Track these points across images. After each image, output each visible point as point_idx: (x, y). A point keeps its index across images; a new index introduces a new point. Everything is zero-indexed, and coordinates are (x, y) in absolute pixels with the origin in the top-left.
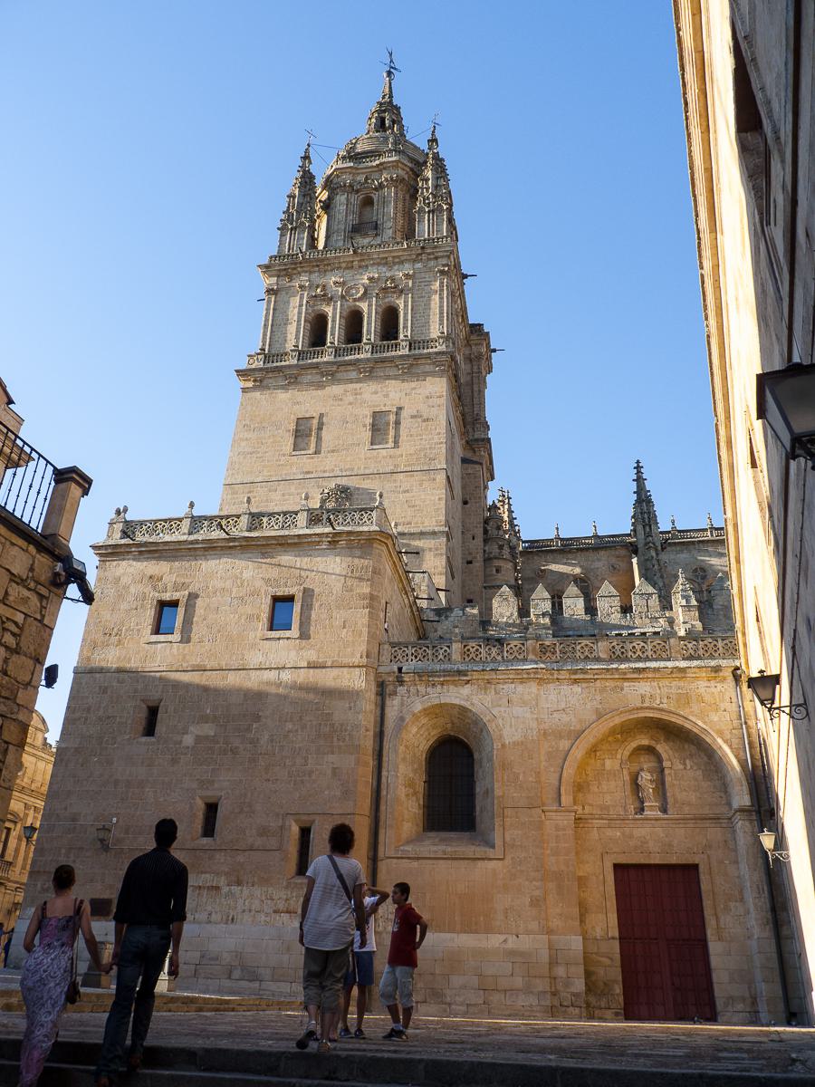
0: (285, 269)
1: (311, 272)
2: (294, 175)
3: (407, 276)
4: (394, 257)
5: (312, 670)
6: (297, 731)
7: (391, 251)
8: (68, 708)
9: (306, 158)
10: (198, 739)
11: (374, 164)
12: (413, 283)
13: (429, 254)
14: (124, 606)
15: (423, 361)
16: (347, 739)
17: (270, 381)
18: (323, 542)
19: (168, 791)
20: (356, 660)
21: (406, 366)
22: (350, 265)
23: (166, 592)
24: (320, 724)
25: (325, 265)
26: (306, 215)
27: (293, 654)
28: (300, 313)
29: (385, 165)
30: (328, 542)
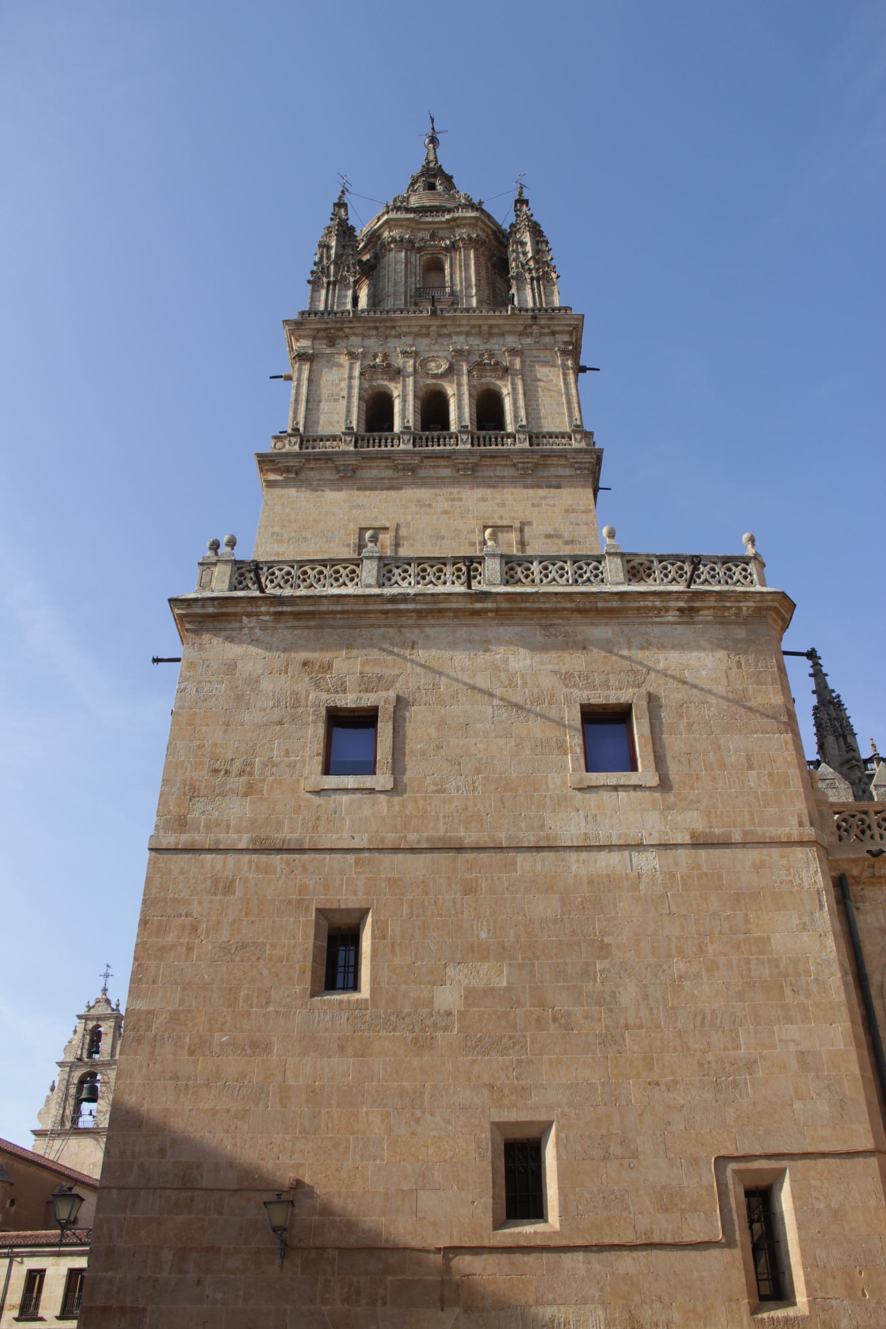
0: (325, 329)
1: (364, 337)
2: (324, 218)
3: (513, 352)
4: (490, 326)
5: (702, 852)
6: (698, 976)
7: (486, 318)
8: (144, 922)
9: (341, 205)
10: (471, 995)
11: (444, 219)
12: (522, 362)
13: (542, 327)
14: (249, 717)
15: (555, 461)
16: (814, 988)
17: (312, 474)
18: (667, 609)
19: (418, 1113)
20: (793, 831)
21: (530, 465)
22: (424, 331)
23: (344, 691)
24: (748, 962)
25: (387, 328)
26: (348, 268)
27: (653, 818)
28: (350, 387)
29: (458, 222)
30: (681, 610)
